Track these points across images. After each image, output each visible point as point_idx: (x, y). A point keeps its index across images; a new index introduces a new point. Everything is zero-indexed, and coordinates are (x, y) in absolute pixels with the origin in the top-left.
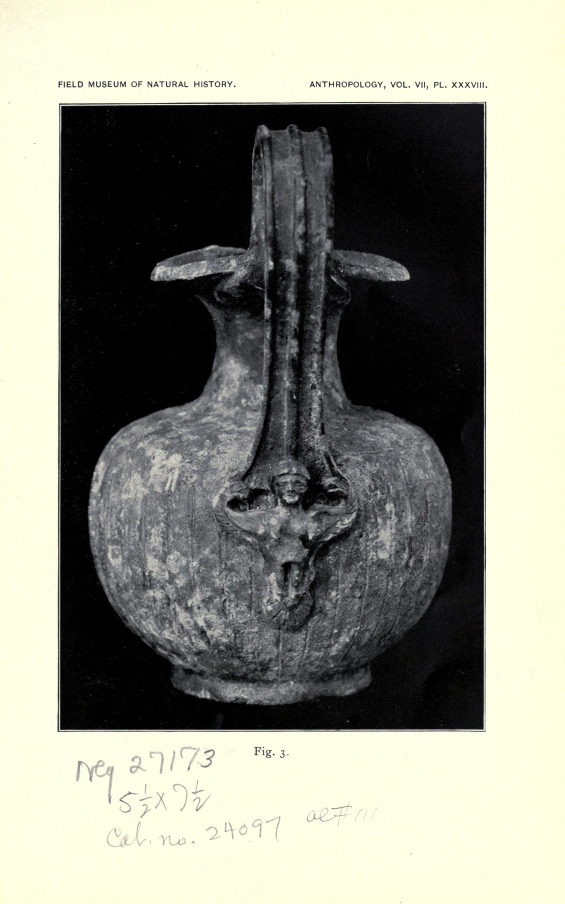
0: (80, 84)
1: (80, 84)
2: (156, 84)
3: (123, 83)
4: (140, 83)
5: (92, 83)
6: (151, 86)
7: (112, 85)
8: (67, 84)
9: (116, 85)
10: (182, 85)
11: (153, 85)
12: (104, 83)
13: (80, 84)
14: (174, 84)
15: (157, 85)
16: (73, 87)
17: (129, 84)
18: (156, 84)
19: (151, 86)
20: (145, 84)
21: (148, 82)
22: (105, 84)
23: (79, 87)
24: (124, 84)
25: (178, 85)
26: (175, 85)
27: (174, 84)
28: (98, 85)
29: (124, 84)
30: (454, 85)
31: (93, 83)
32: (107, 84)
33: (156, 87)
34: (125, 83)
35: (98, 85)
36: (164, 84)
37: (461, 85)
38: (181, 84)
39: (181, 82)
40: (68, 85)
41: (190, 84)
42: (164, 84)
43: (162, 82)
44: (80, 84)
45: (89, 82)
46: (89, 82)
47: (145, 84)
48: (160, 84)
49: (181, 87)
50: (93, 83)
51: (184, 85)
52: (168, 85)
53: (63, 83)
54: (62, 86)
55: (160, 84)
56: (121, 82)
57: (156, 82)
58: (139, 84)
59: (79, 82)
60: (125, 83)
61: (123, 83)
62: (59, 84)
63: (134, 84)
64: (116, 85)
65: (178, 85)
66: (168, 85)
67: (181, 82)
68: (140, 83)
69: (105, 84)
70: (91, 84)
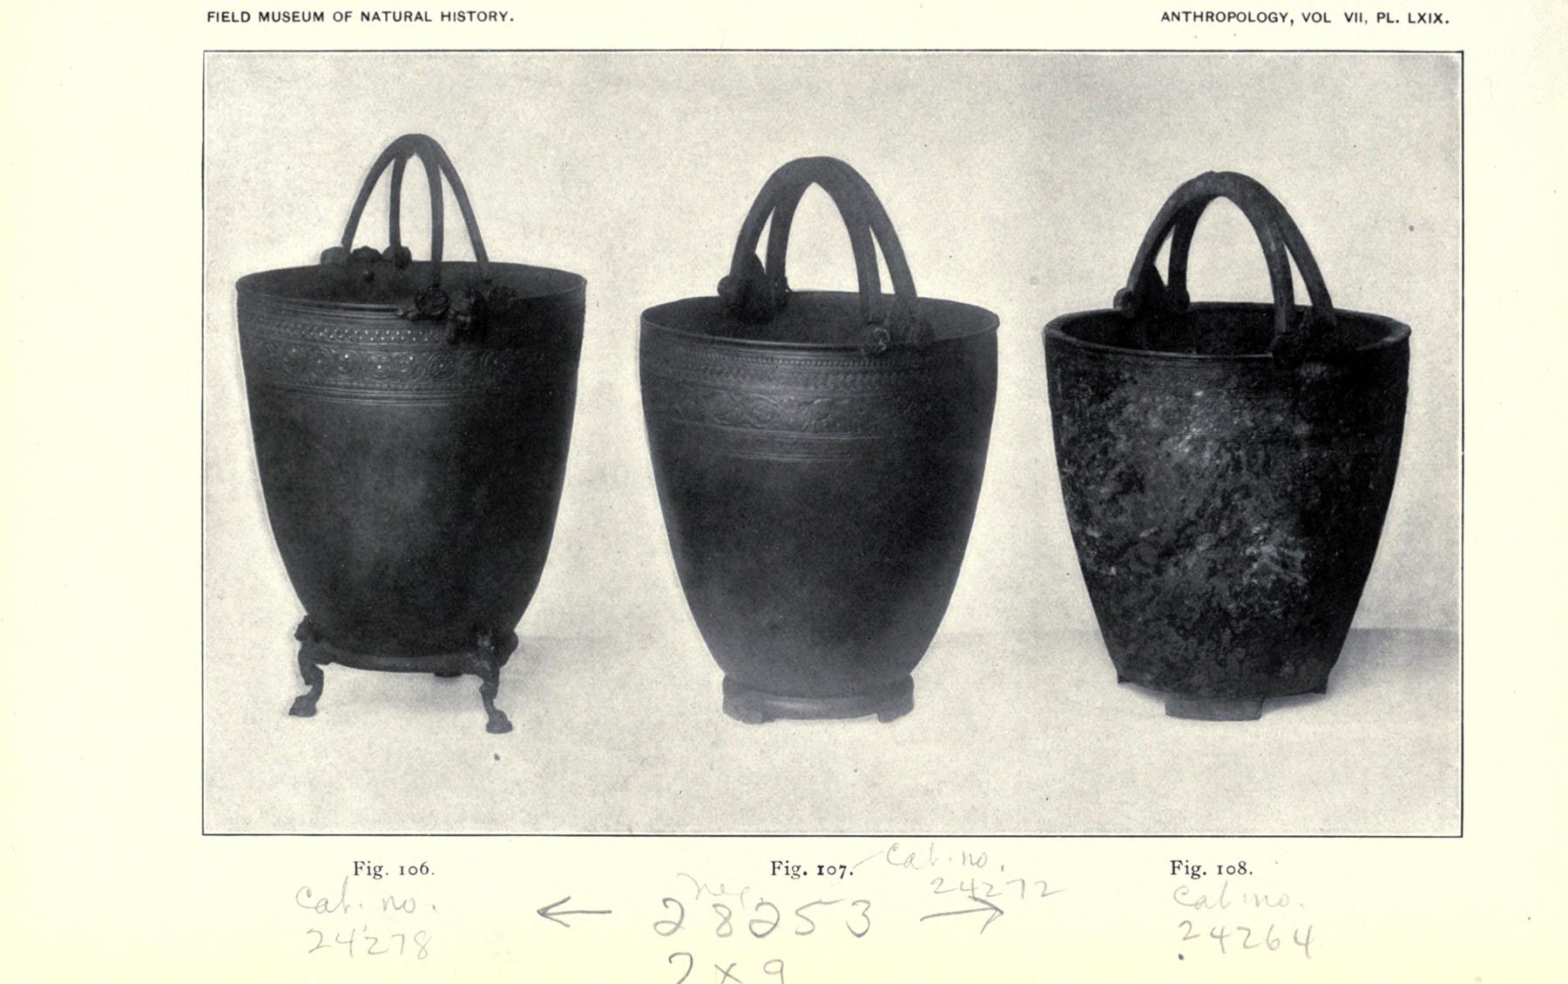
1: (245, 17)
2: (376, 16)
3: (319, 14)
5: (264, 14)
6: (368, 19)
7: (300, 18)
8: (223, 17)
9: (306, 17)
10: (421, 18)
11: (371, 17)
12: (286, 15)
14: (408, 16)
15: (378, 18)
16: (234, 21)
17: (328, 17)
18: (376, 16)
19: (368, 19)
21: (363, 14)
23: (243, 21)
25: (413, 17)
26: (410, 17)
27: (408, 16)
28: (276, 18)
30: (1422, 18)
31: (268, 14)
32: (291, 16)
33: (376, 21)
34: (322, 14)
35: (276, 18)
37: (1422, 18)
38: (419, 17)
39: (419, 13)
41: (434, 15)
43: (386, 13)
45: (261, 14)
46: (261, 14)
47: (356, 16)
48: (382, 16)
49: (419, 21)
50: (268, 14)
51: (423, 17)
52: (397, 18)
53: (215, 15)
54: (213, 20)
55: (382, 16)
56: (315, 14)
57: (376, 14)
58: (347, 17)
59: (243, 13)
60: (322, 14)
61: (319, 14)
62: (209, 17)
63: (338, 17)
64: (306, 17)
66: (397, 18)
67: (419, 13)
70: (264, 17)
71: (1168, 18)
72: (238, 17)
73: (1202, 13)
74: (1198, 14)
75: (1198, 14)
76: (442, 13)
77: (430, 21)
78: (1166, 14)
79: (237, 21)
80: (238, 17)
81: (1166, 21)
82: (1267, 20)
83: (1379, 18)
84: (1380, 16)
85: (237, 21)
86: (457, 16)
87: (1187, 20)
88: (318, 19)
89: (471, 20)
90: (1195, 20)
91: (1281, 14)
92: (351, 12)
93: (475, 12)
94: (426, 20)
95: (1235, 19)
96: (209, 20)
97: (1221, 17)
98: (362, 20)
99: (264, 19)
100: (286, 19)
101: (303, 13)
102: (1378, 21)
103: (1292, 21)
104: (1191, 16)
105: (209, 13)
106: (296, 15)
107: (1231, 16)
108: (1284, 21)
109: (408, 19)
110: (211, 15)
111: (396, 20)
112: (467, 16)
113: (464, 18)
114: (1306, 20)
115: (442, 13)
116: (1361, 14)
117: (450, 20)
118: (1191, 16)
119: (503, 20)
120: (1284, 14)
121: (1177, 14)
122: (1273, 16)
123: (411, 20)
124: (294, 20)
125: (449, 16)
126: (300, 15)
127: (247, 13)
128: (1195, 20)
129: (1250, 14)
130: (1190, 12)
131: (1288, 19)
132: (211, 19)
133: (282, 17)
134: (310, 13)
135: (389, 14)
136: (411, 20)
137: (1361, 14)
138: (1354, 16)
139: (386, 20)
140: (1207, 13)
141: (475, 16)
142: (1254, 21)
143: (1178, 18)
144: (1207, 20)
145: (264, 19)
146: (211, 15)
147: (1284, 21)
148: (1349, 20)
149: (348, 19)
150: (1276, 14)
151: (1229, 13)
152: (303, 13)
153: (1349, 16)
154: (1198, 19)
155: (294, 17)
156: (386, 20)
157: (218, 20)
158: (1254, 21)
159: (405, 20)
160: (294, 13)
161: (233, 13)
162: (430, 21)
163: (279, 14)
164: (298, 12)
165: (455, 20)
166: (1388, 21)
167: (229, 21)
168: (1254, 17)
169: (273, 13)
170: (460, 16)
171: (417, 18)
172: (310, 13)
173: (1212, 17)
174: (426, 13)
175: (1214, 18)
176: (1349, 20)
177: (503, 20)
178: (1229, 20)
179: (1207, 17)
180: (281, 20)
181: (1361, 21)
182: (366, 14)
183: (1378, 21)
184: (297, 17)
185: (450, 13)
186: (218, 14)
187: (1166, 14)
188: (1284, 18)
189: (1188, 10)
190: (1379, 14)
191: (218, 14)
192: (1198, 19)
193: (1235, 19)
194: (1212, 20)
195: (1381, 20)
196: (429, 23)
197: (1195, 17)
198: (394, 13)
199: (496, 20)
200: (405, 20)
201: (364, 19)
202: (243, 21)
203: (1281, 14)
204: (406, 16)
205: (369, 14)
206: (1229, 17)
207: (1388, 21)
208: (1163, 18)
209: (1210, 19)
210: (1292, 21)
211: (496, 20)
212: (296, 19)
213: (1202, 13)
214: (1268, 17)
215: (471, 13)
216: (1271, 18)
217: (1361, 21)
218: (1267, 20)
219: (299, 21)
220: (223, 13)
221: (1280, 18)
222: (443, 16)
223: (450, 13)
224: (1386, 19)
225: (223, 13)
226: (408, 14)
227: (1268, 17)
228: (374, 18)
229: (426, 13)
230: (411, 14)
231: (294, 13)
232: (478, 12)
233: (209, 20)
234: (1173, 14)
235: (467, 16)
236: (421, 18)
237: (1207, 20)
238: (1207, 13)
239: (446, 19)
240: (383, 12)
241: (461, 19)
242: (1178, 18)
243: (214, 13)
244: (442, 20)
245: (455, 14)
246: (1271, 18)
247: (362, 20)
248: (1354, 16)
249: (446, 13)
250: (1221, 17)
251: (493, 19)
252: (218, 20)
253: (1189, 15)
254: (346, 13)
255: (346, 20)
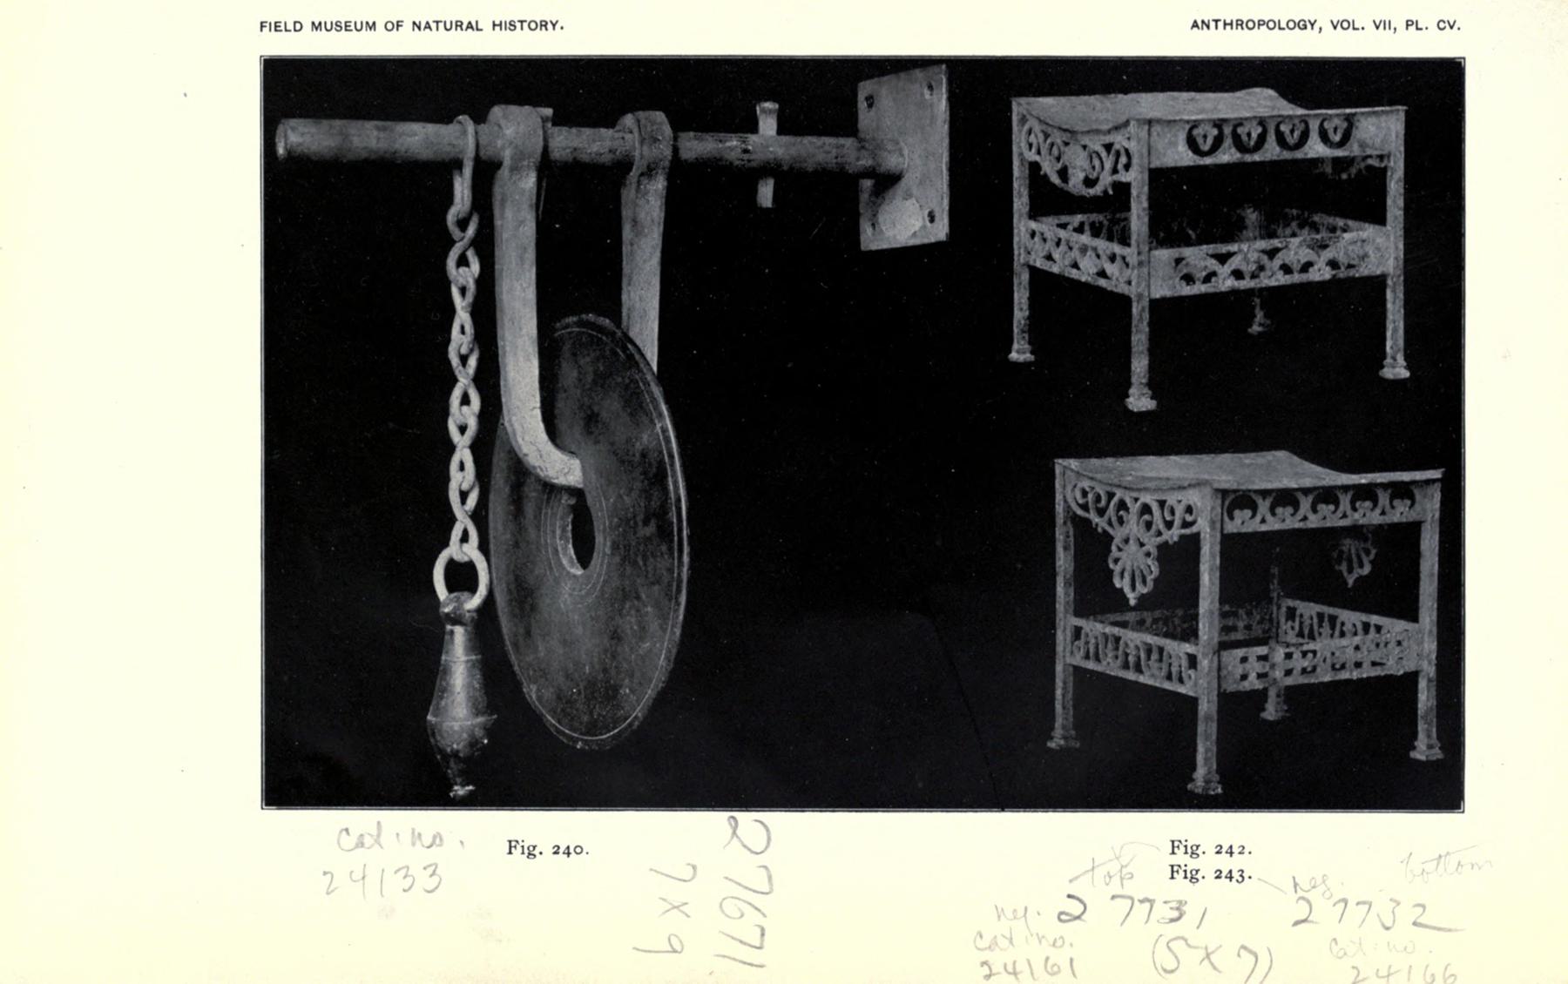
0: (298, 26)
1: (298, 26)
3: (371, 24)
4: (399, 25)
5: (317, 24)
6: (419, 28)
7: (353, 27)
9: (359, 27)
10: (472, 27)
11: (422, 27)
12: (338, 24)
13: (298, 27)
14: (459, 25)
15: (430, 28)
17: (380, 26)
18: (428, 26)
19: (419, 28)
20: (408, 25)
21: (414, 23)
22: (338, 26)
24: (372, 26)
25: (464, 27)
26: (461, 26)
27: (459, 25)
28: (329, 27)
29: (372, 26)
31: (320, 24)
32: (343, 25)
33: (428, 30)
34: (374, 23)
35: (329, 27)
36: (441, 25)
38: (470, 26)
39: (470, 23)
40: (277, 27)
41: (486, 25)
42: (441, 25)
43: (437, 22)
44: (298, 27)
45: (313, 23)
46: (313, 23)
47: (408, 25)
48: (433, 26)
49: (470, 30)
50: (320, 24)
51: (475, 27)
52: (448, 27)
53: (268, 25)
54: (266, 30)
55: (433, 26)
56: (367, 23)
57: (427, 23)
58: (398, 26)
59: (295, 23)
60: (374, 23)
61: (371, 24)
62: (262, 27)
63: (390, 26)
64: (359, 27)
65: (464, 27)
66: (448, 27)
68: (399, 25)
69: (338, 26)
70: (316, 26)
71: (1197, 26)
72: (290, 26)
73: (1232, 21)
74: (1228, 21)
75: (1228, 21)
76: (494, 22)
77: (481, 30)
78: (1195, 22)
79: (290, 31)
80: (290, 26)
81: (1195, 29)
82: (1297, 28)
83: (1407, 25)
84: (1408, 24)
85: (290, 31)
86: (508, 25)
87: (1217, 28)
88: (371, 29)
89: (522, 29)
90: (1225, 28)
91: (1310, 21)
92: (402, 22)
93: (525, 21)
94: (478, 29)
95: (1265, 26)
96: (261, 30)
97: (1251, 25)
98: (413, 30)
99: (317, 29)
100: (339, 28)
101: (355, 23)
102: (1407, 29)
103: (1321, 29)
104: (1221, 24)
105: (262, 23)
106: (348, 24)
107: (1261, 23)
108: (1312, 28)
109: (459, 28)
110: (264, 24)
111: (446, 29)
112: (518, 25)
113: (515, 27)
114: (1335, 28)
115: (494, 22)
116: (1390, 22)
117: (501, 29)
118: (1221, 24)
119: (554, 29)
120: (1312, 21)
121: (1206, 22)
122: (1302, 23)
123: (462, 29)
124: (346, 30)
125: (500, 25)
126: (353, 24)
127: (299, 22)
128: (1225, 28)
129: (1279, 21)
130: (1220, 20)
131: (1316, 27)
132: (264, 29)
133: (334, 26)
134: (362, 23)
135: (440, 24)
136: (462, 29)
137: (1390, 22)
138: (1382, 24)
139: (437, 29)
140: (1237, 21)
141: (525, 25)
142: (1284, 29)
143: (1208, 27)
144: (1237, 28)
145: (317, 29)
146: (264, 24)
147: (1312, 28)
148: (1377, 28)
149: (400, 28)
150: (1305, 21)
151: (1259, 21)
152: (355, 23)
153: (1378, 24)
154: (1228, 27)
155: (346, 26)
156: (437, 29)
157: (270, 30)
158: (1284, 29)
159: (456, 29)
160: (346, 22)
161: (285, 23)
162: (481, 30)
163: (332, 23)
164: (350, 22)
165: (506, 29)
166: (1417, 29)
167: (281, 31)
168: (1283, 25)
169: (325, 23)
170: (511, 25)
171: (468, 28)
172: (362, 23)
173: (1241, 25)
174: (477, 22)
175: (1244, 25)
176: (1377, 28)
177: (554, 29)
178: (1259, 28)
179: (1237, 25)
180: (334, 30)
181: (1390, 28)
182: (418, 23)
183: (1407, 29)
184: (350, 26)
185: (501, 22)
186: (270, 24)
187: (1195, 22)
188: (1312, 25)
189: (1216, 18)
190: (1407, 21)
191: (270, 24)
192: (1228, 27)
193: (1265, 26)
194: (1242, 28)
195: (1409, 27)
196: (480, 32)
197: (1225, 24)
198: (445, 23)
199: (546, 29)
200: (456, 29)
201: (416, 28)
202: (295, 30)
203: (1310, 21)
204: (457, 26)
205: (420, 22)
206: (1259, 25)
207: (1417, 29)
208: (1193, 26)
209: (1239, 27)
210: (1321, 29)
211: (546, 29)
212: (348, 28)
213: (1232, 21)
214: (1297, 25)
215: (522, 22)
216: (1302, 25)
217: (1390, 28)
218: (1297, 28)
219: (351, 30)
220: (276, 23)
221: (1309, 26)
222: (494, 25)
223: (501, 22)
224: (1414, 25)
225: (276, 23)
226: (459, 24)
227: (1297, 25)
228: (426, 27)
229: (477, 22)
230: (462, 23)
231: (346, 22)
232: (528, 21)
233: (261, 30)
234: (1203, 22)
235: (518, 25)
236: (472, 27)
237: (1237, 28)
238: (1237, 21)
239: (497, 28)
240: (434, 22)
241: (512, 28)
242: (1208, 27)
243: (266, 22)
244: (494, 29)
245: (506, 22)
246: (1302, 25)
247: (413, 30)
248: (1382, 24)
249: (497, 22)
250: (1251, 25)
251: (543, 28)
252: (270, 30)
253: (1219, 23)
254: (398, 22)
255: (397, 29)
